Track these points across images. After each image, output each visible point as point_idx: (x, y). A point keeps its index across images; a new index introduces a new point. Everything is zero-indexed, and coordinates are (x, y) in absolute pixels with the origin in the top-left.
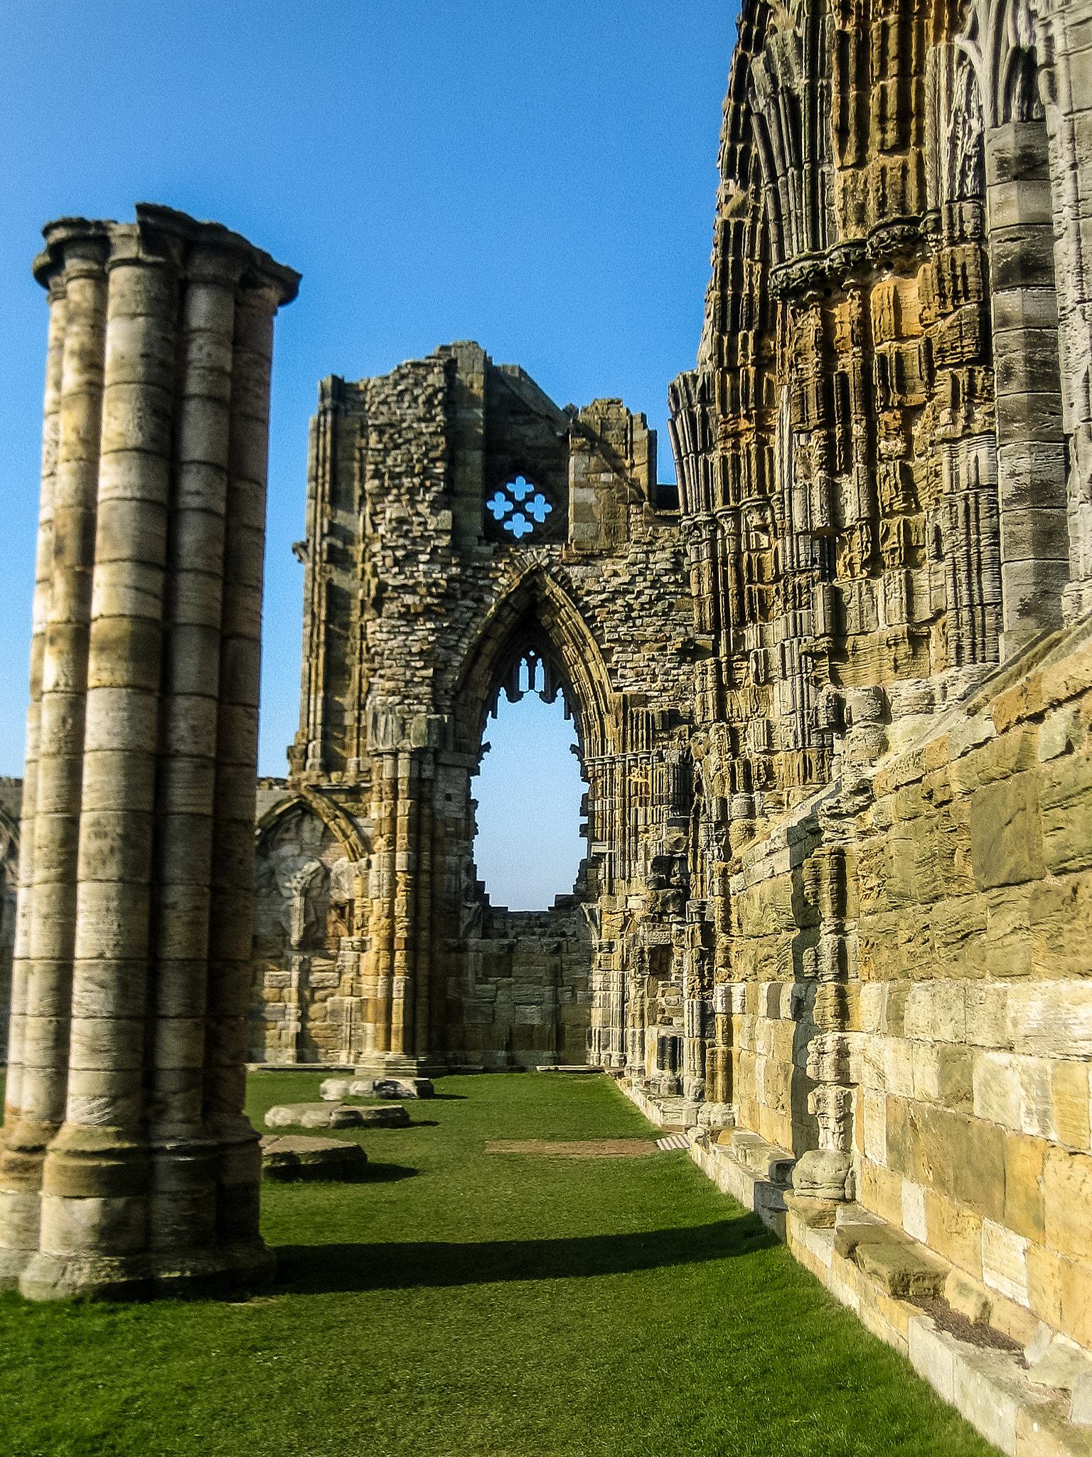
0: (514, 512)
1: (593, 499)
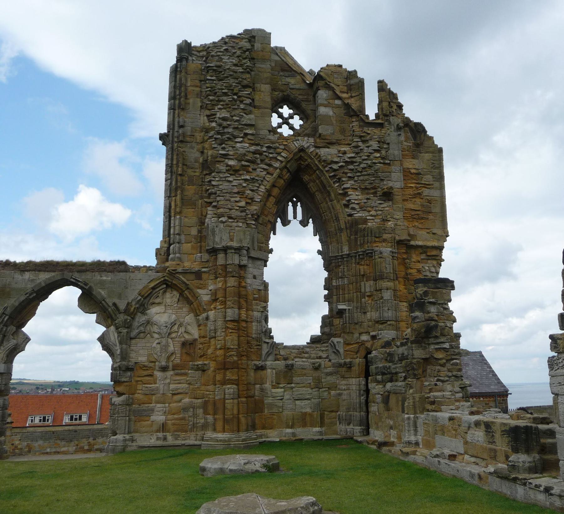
0: (283, 123)
1: (331, 113)
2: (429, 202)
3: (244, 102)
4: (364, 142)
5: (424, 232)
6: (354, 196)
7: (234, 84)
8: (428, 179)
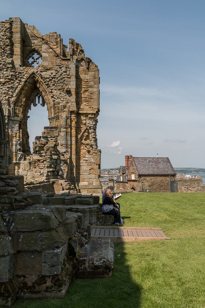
2: (92, 94)
3: (7, 53)
4: (60, 68)
5: (88, 107)
6: (55, 92)
7: (2, 45)
8: (92, 83)
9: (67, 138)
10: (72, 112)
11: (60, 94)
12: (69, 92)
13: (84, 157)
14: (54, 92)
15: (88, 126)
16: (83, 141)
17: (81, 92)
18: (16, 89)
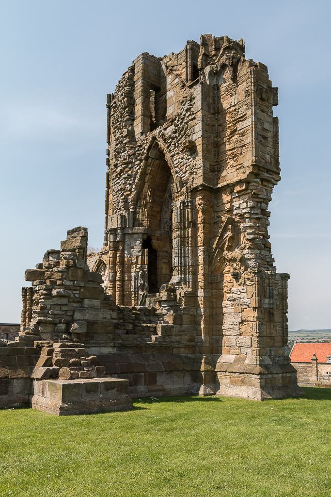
5: (235, 169)
9: (185, 251)
10: (194, 191)
11: (182, 158)
12: (191, 149)
13: (228, 293)
14: (176, 160)
15: (236, 215)
16: (226, 254)
17: (225, 139)
18: (135, 178)
